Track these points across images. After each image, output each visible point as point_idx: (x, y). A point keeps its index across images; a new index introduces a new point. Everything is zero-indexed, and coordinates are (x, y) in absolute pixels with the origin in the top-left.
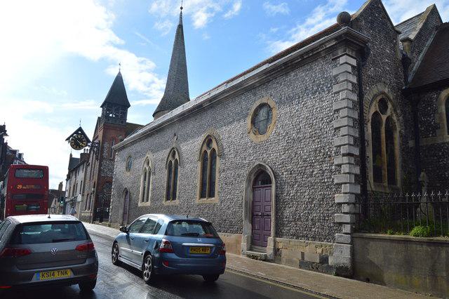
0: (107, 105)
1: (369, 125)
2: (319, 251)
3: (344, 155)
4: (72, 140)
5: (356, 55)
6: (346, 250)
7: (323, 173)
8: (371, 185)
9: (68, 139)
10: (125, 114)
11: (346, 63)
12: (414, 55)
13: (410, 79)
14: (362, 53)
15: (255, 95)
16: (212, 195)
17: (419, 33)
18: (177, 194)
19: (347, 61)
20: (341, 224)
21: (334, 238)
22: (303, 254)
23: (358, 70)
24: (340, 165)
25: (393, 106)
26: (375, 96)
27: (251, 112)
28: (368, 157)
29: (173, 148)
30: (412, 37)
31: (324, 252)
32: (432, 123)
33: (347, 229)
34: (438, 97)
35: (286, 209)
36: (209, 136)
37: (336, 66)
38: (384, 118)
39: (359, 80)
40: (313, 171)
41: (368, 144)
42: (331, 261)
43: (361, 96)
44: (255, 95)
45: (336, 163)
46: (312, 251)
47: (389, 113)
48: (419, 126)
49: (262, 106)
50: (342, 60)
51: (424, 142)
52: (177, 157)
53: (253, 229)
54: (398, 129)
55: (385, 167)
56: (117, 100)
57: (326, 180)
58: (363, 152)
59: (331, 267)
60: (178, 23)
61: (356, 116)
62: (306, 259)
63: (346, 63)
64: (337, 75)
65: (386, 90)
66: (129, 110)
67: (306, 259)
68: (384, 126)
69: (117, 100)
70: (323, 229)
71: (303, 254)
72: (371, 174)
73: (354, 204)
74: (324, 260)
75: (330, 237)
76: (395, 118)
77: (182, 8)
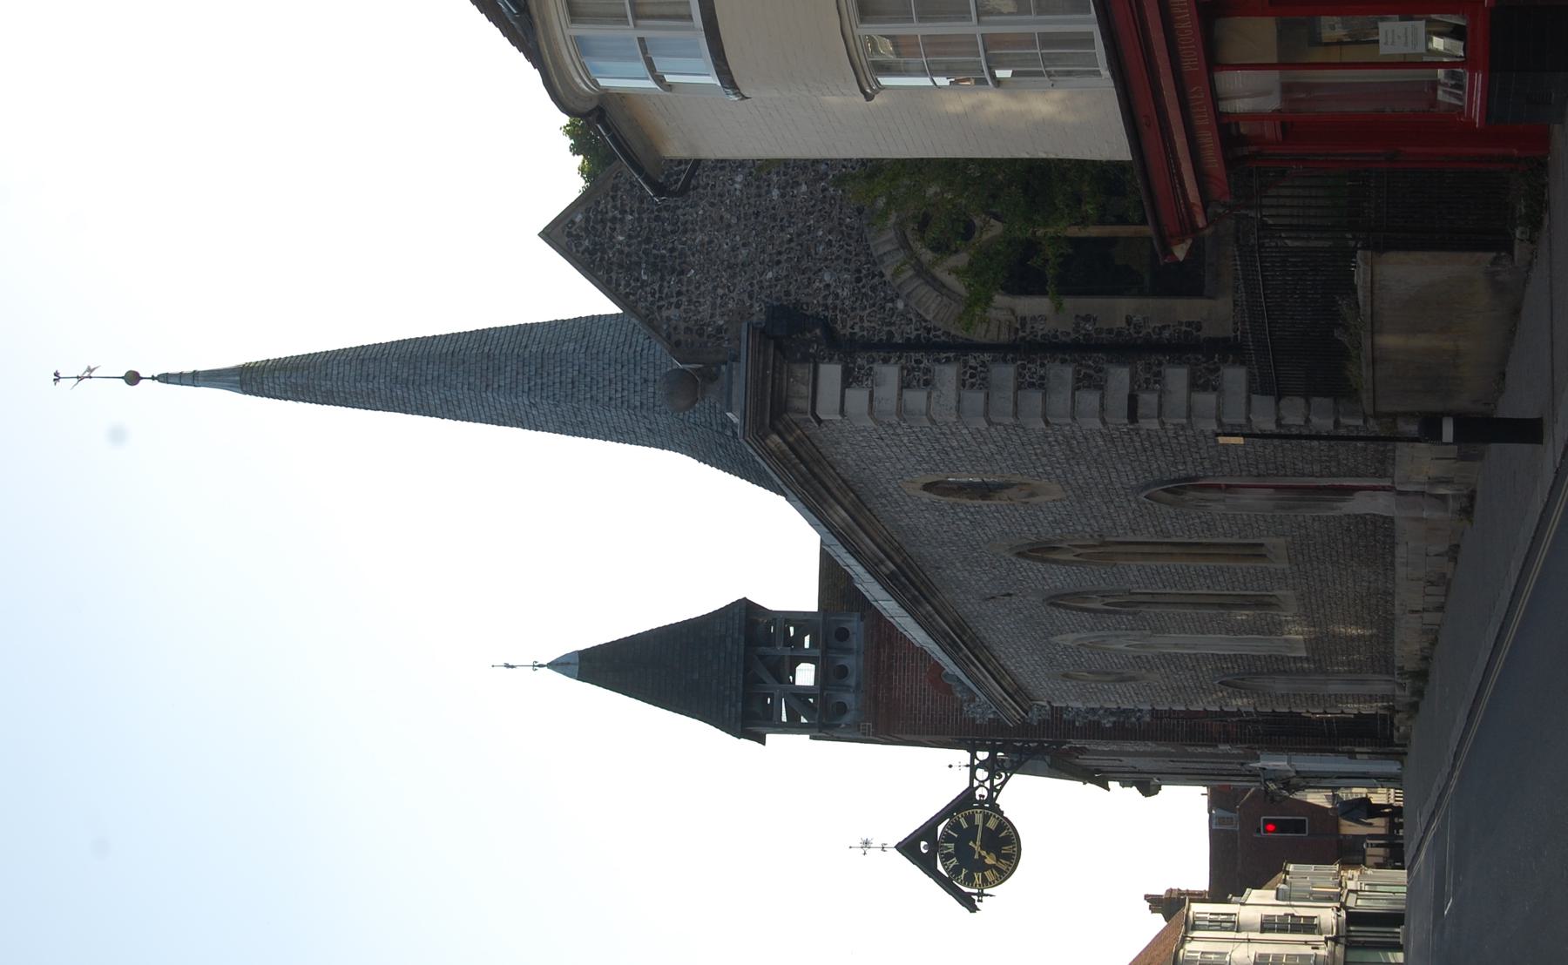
0: (747, 717)
3: (1133, 415)
4: (969, 881)
8: (1214, 313)
9: (969, 903)
11: (842, 411)
28: (1129, 320)
36: (1020, 554)
39: (887, 348)
41: (1087, 318)
56: (712, 670)
58: (1123, 348)
61: (1004, 373)
69: (712, 670)
72: (1185, 310)
77: (133, 378)
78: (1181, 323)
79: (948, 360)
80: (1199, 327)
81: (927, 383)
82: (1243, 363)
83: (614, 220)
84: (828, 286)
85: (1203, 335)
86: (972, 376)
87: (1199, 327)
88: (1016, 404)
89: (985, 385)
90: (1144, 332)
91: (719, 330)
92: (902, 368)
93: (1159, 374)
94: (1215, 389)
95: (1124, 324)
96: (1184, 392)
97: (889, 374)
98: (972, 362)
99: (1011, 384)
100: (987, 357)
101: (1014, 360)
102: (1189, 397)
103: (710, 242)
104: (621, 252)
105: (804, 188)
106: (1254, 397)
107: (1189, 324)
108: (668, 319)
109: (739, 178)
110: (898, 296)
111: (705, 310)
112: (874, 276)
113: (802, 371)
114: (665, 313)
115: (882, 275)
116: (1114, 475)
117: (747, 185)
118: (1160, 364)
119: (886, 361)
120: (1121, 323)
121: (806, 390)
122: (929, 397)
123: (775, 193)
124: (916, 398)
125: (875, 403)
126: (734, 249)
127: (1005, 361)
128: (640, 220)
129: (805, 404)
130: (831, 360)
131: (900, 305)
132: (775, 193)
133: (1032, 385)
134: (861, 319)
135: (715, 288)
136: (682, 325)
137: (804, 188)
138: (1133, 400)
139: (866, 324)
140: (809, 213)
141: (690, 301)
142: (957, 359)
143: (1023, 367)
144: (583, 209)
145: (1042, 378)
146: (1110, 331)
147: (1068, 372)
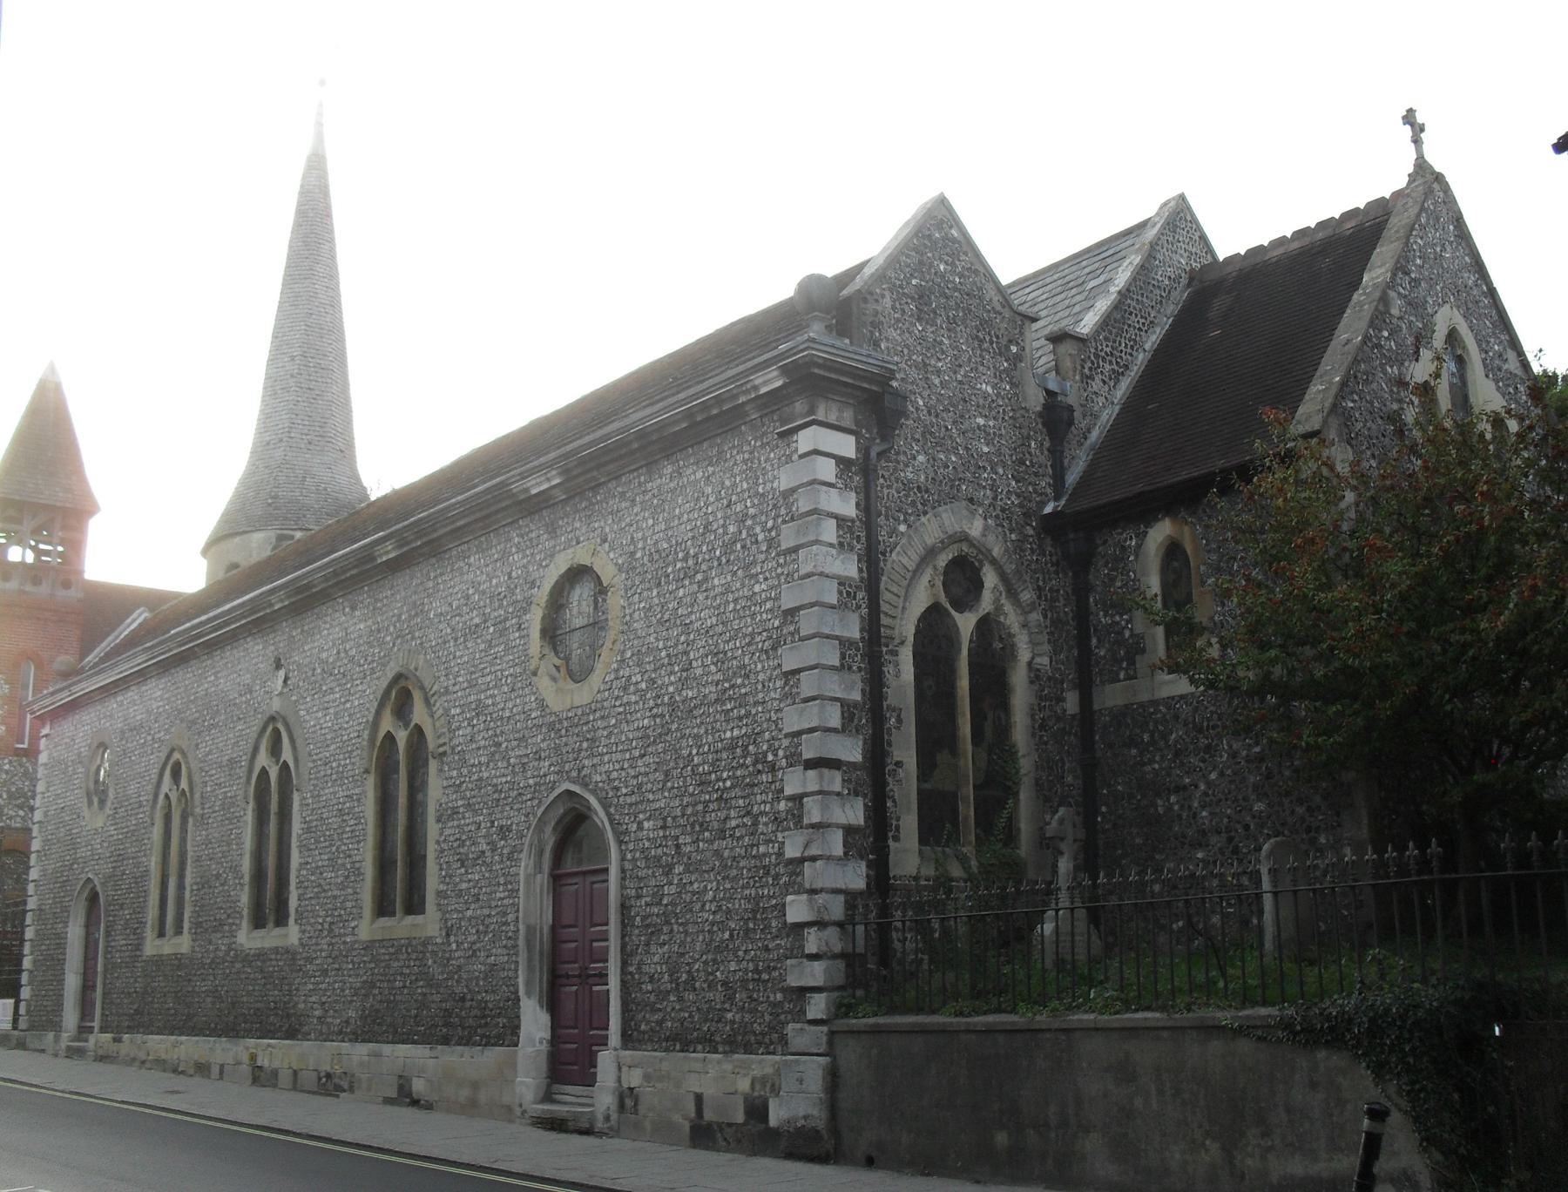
1: (906, 656)
2: (744, 1085)
3: (811, 764)
5: (857, 422)
6: (813, 1071)
7: (755, 824)
8: (907, 857)
10: (74, 546)
12: (1096, 385)
13: (1072, 478)
14: (877, 406)
15: (552, 531)
16: (414, 905)
17: (1116, 306)
18: (293, 903)
19: (829, 442)
20: (803, 991)
21: (783, 1040)
22: (699, 1099)
23: (861, 472)
24: (798, 799)
25: (1003, 576)
26: (930, 553)
27: (542, 594)
28: (899, 764)
29: (272, 719)
30: (1087, 324)
31: (758, 1087)
32: (1127, 634)
33: (817, 1006)
34: (1139, 546)
35: (653, 949)
36: (399, 677)
37: (789, 460)
38: (966, 623)
40: (727, 818)
41: (899, 721)
42: (777, 1115)
43: (872, 560)
44: (552, 531)
45: (788, 791)
46: (719, 1079)
47: (986, 603)
48: (1094, 641)
49: (578, 573)
50: (806, 440)
51: (1110, 697)
52: (287, 755)
53: (555, 1026)
54: (1024, 655)
55: (969, 791)
57: (762, 849)
59: (775, 1133)
60: (305, 151)
61: (853, 631)
62: (708, 1115)
63: (817, 452)
64: (793, 490)
65: (976, 528)
66: (95, 529)
67: (708, 1115)
68: (965, 652)
70: (753, 1011)
71: (699, 1099)
72: (909, 823)
73: (840, 925)
74: (757, 1111)
75: (772, 1040)
76: (1012, 619)
78: (898, 819)
79: (860, 570)
80: (896, 839)
81: (841, 544)
82: (868, 885)
83: (953, 264)
84: (915, 458)
85: (891, 842)
86: (848, 593)
87: (896, 839)
88: (828, 637)
89: (842, 606)
90: (890, 780)
91: (876, 344)
92: (853, 521)
93: (857, 795)
94: (846, 854)
95: (896, 759)
96: (843, 820)
97: (847, 506)
98: (860, 595)
99: (846, 634)
100: (865, 611)
101: (862, 638)
102: (838, 826)
103: (943, 352)
104: (931, 265)
105: (986, 449)
106: (842, 898)
107: (897, 828)
108: (883, 296)
109: (989, 389)
110: (909, 526)
111: (893, 334)
112: (924, 505)
113: (848, 418)
114: (887, 293)
115: (925, 513)
116: (619, 756)
117: (986, 396)
118: (865, 796)
119: (858, 505)
120: (897, 755)
121: (832, 419)
122: (831, 545)
123: (981, 421)
124: (829, 531)
125: (825, 488)
126: (938, 372)
127: (861, 631)
128: (955, 289)
129: (820, 416)
130: (857, 449)
131: (902, 528)
132: (981, 421)
133: (843, 657)
134: (889, 487)
135: (907, 346)
136: (879, 309)
137: (986, 449)
138: (833, 764)
139: (886, 491)
140: (967, 449)
141: (898, 320)
142: (862, 580)
143: (858, 649)
144: (961, 238)
145: (850, 668)
146: (890, 744)
147: (856, 696)
